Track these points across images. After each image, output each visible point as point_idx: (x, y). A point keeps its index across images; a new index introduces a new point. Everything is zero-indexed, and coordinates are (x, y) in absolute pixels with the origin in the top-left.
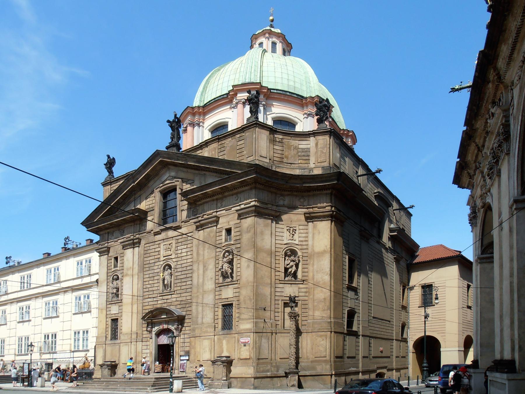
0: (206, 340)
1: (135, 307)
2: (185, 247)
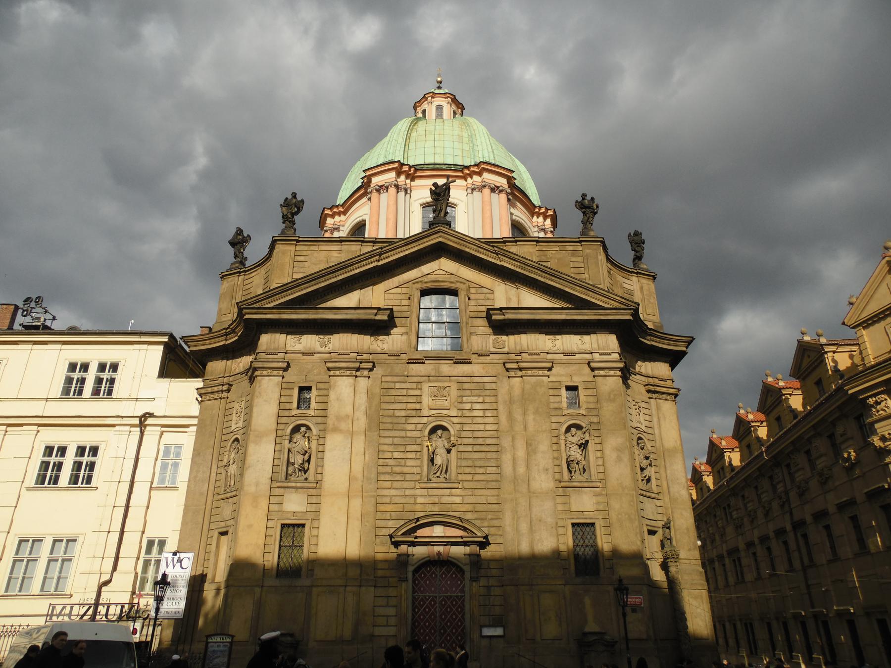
1: (356, 503)
2: (480, 400)
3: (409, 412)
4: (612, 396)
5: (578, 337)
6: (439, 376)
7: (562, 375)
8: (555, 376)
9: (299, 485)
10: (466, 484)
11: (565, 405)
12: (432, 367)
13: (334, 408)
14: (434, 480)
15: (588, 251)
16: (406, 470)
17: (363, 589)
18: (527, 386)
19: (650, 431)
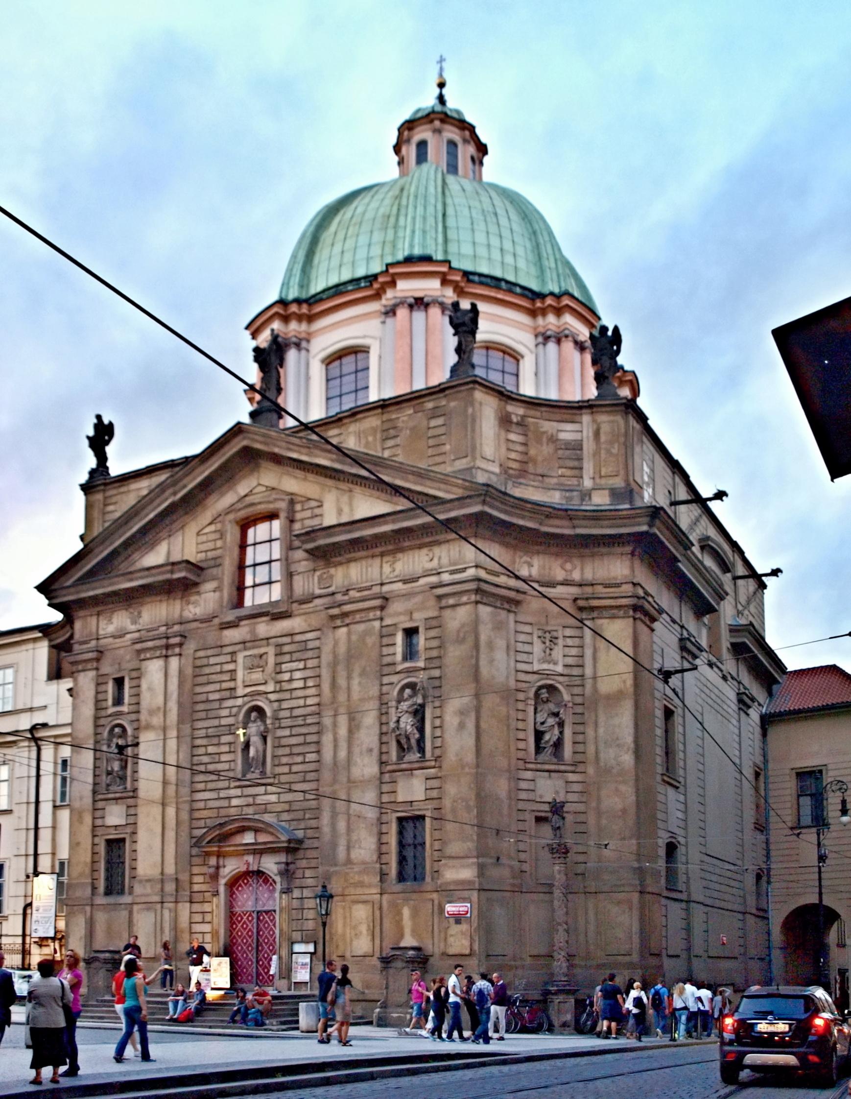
0: (360, 906)
1: (171, 811)
2: (301, 665)
3: (224, 693)
5: (425, 551)
6: (255, 641)
7: (400, 614)
9: (118, 795)
11: (399, 657)
15: (453, 404)
16: (220, 767)
17: (180, 905)
18: (354, 638)
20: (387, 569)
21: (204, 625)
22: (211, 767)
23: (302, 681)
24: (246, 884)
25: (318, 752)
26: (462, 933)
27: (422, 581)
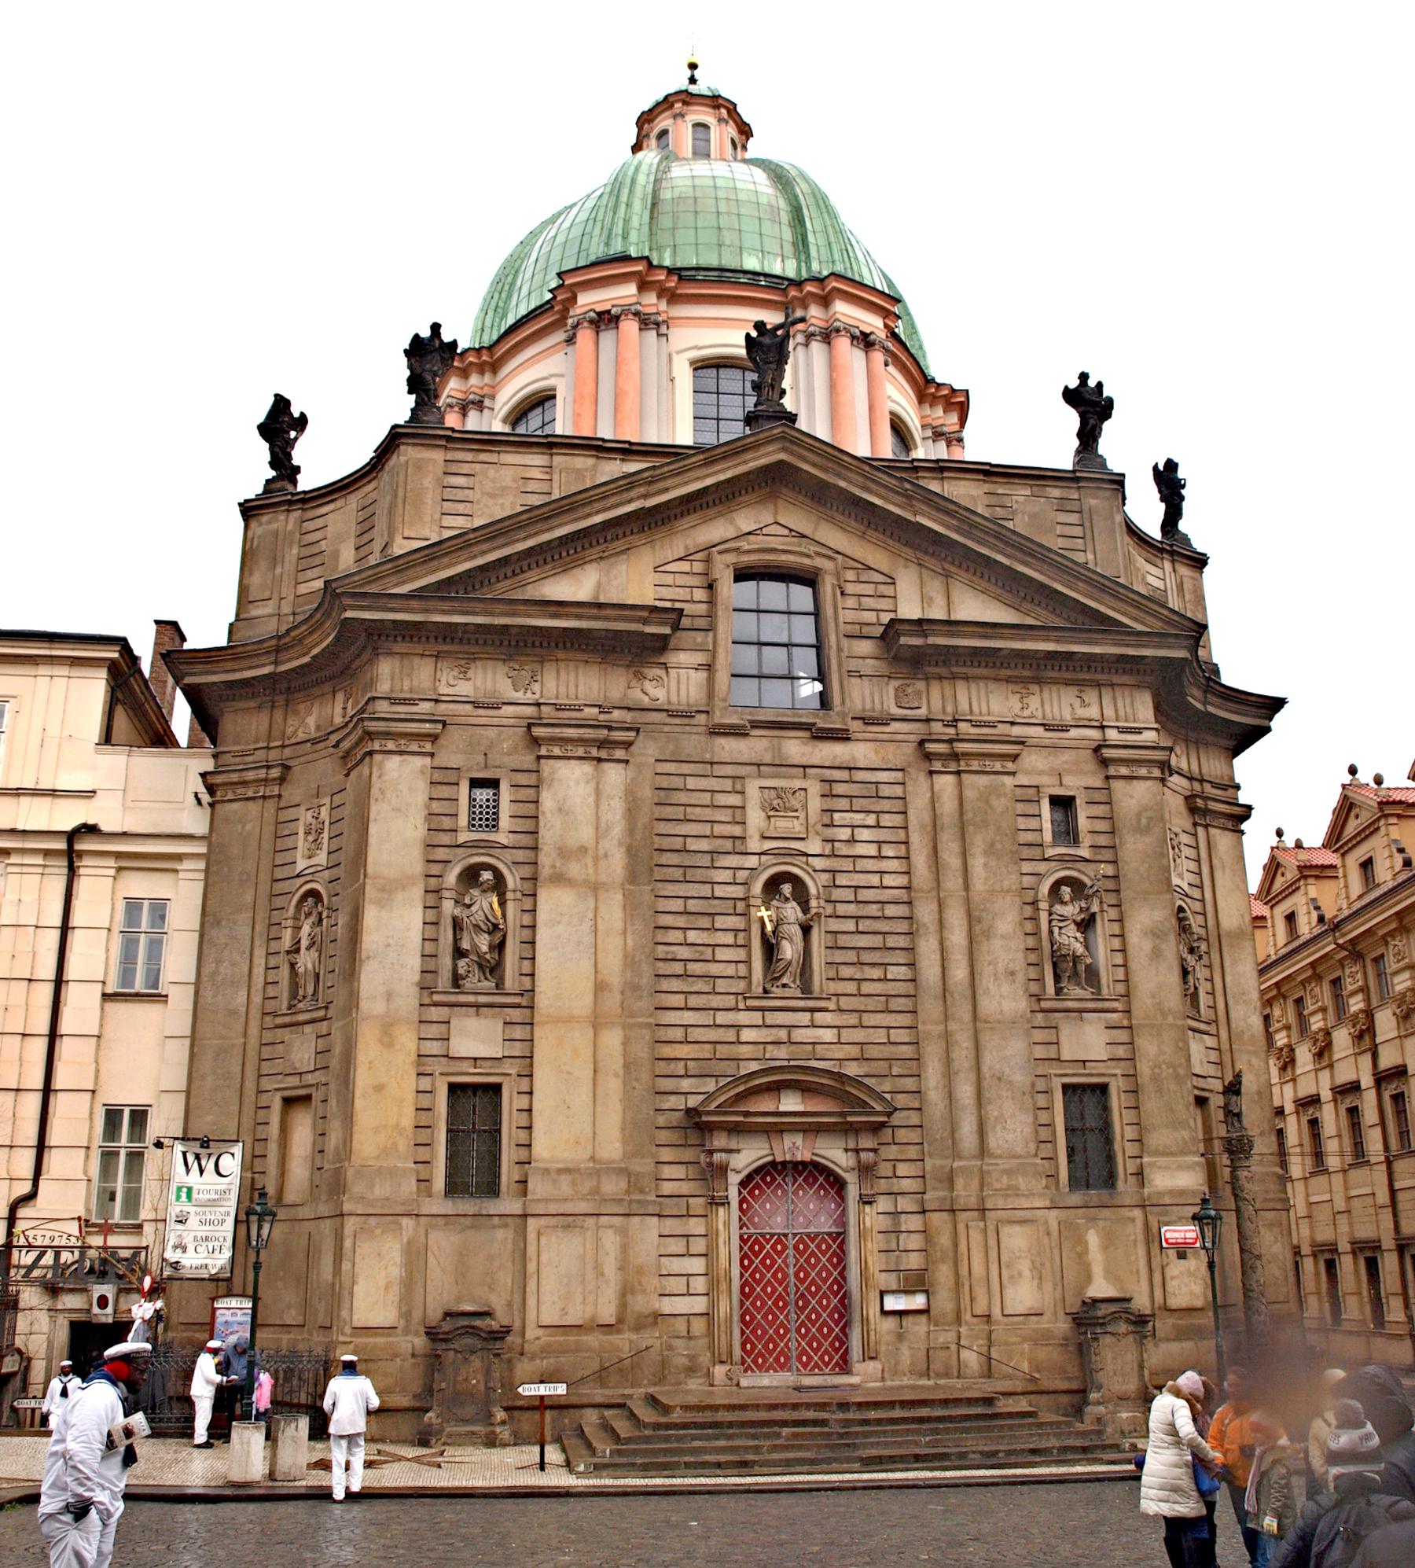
0: (1017, 1228)
1: (612, 1039)
2: (871, 820)
3: (720, 841)
4: (1144, 821)
5: (1073, 691)
6: (781, 766)
7: (1041, 773)
8: (1027, 773)
9: (482, 999)
10: (845, 1003)
11: (1048, 836)
12: (765, 743)
13: (551, 831)
14: (777, 991)
15: (1093, 502)
16: (715, 969)
19: (1196, 893)
20: (1014, 703)
21: (678, 721)
22: (693, 968)
23: (875, 846)
24: (768, 1185)
25: (912, 965)
26: (1190, 1273)
27: (1074, 733)
